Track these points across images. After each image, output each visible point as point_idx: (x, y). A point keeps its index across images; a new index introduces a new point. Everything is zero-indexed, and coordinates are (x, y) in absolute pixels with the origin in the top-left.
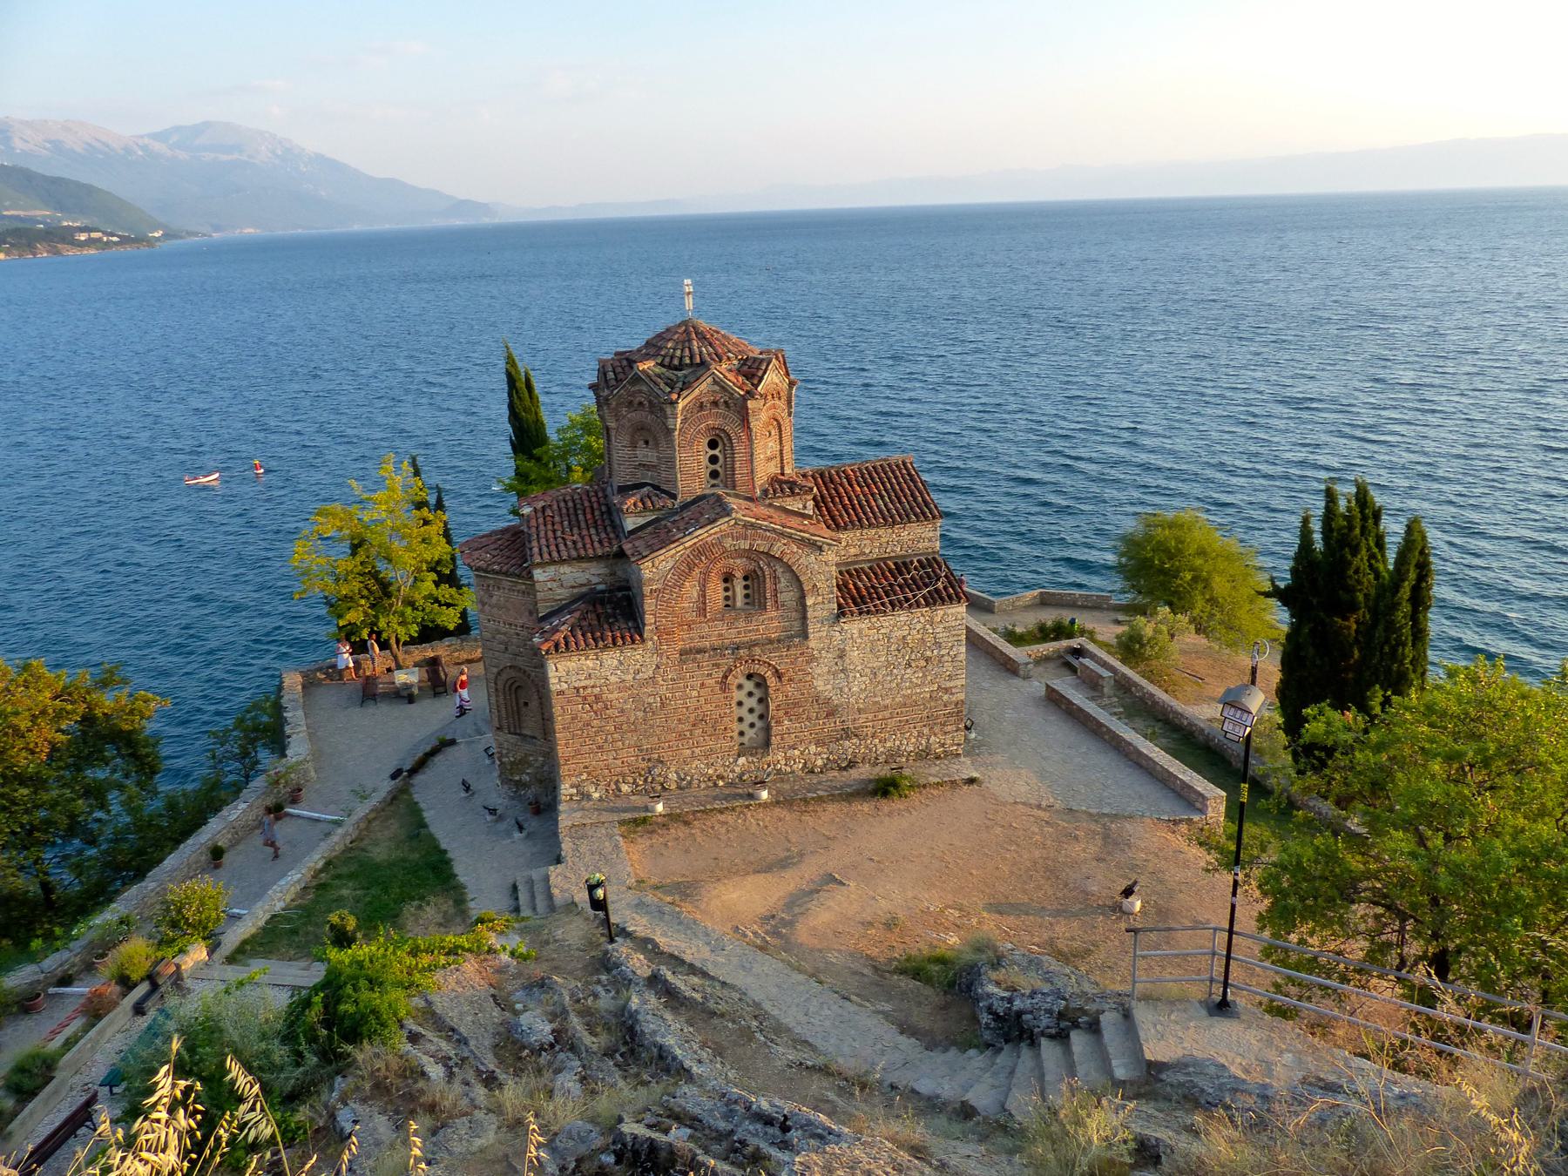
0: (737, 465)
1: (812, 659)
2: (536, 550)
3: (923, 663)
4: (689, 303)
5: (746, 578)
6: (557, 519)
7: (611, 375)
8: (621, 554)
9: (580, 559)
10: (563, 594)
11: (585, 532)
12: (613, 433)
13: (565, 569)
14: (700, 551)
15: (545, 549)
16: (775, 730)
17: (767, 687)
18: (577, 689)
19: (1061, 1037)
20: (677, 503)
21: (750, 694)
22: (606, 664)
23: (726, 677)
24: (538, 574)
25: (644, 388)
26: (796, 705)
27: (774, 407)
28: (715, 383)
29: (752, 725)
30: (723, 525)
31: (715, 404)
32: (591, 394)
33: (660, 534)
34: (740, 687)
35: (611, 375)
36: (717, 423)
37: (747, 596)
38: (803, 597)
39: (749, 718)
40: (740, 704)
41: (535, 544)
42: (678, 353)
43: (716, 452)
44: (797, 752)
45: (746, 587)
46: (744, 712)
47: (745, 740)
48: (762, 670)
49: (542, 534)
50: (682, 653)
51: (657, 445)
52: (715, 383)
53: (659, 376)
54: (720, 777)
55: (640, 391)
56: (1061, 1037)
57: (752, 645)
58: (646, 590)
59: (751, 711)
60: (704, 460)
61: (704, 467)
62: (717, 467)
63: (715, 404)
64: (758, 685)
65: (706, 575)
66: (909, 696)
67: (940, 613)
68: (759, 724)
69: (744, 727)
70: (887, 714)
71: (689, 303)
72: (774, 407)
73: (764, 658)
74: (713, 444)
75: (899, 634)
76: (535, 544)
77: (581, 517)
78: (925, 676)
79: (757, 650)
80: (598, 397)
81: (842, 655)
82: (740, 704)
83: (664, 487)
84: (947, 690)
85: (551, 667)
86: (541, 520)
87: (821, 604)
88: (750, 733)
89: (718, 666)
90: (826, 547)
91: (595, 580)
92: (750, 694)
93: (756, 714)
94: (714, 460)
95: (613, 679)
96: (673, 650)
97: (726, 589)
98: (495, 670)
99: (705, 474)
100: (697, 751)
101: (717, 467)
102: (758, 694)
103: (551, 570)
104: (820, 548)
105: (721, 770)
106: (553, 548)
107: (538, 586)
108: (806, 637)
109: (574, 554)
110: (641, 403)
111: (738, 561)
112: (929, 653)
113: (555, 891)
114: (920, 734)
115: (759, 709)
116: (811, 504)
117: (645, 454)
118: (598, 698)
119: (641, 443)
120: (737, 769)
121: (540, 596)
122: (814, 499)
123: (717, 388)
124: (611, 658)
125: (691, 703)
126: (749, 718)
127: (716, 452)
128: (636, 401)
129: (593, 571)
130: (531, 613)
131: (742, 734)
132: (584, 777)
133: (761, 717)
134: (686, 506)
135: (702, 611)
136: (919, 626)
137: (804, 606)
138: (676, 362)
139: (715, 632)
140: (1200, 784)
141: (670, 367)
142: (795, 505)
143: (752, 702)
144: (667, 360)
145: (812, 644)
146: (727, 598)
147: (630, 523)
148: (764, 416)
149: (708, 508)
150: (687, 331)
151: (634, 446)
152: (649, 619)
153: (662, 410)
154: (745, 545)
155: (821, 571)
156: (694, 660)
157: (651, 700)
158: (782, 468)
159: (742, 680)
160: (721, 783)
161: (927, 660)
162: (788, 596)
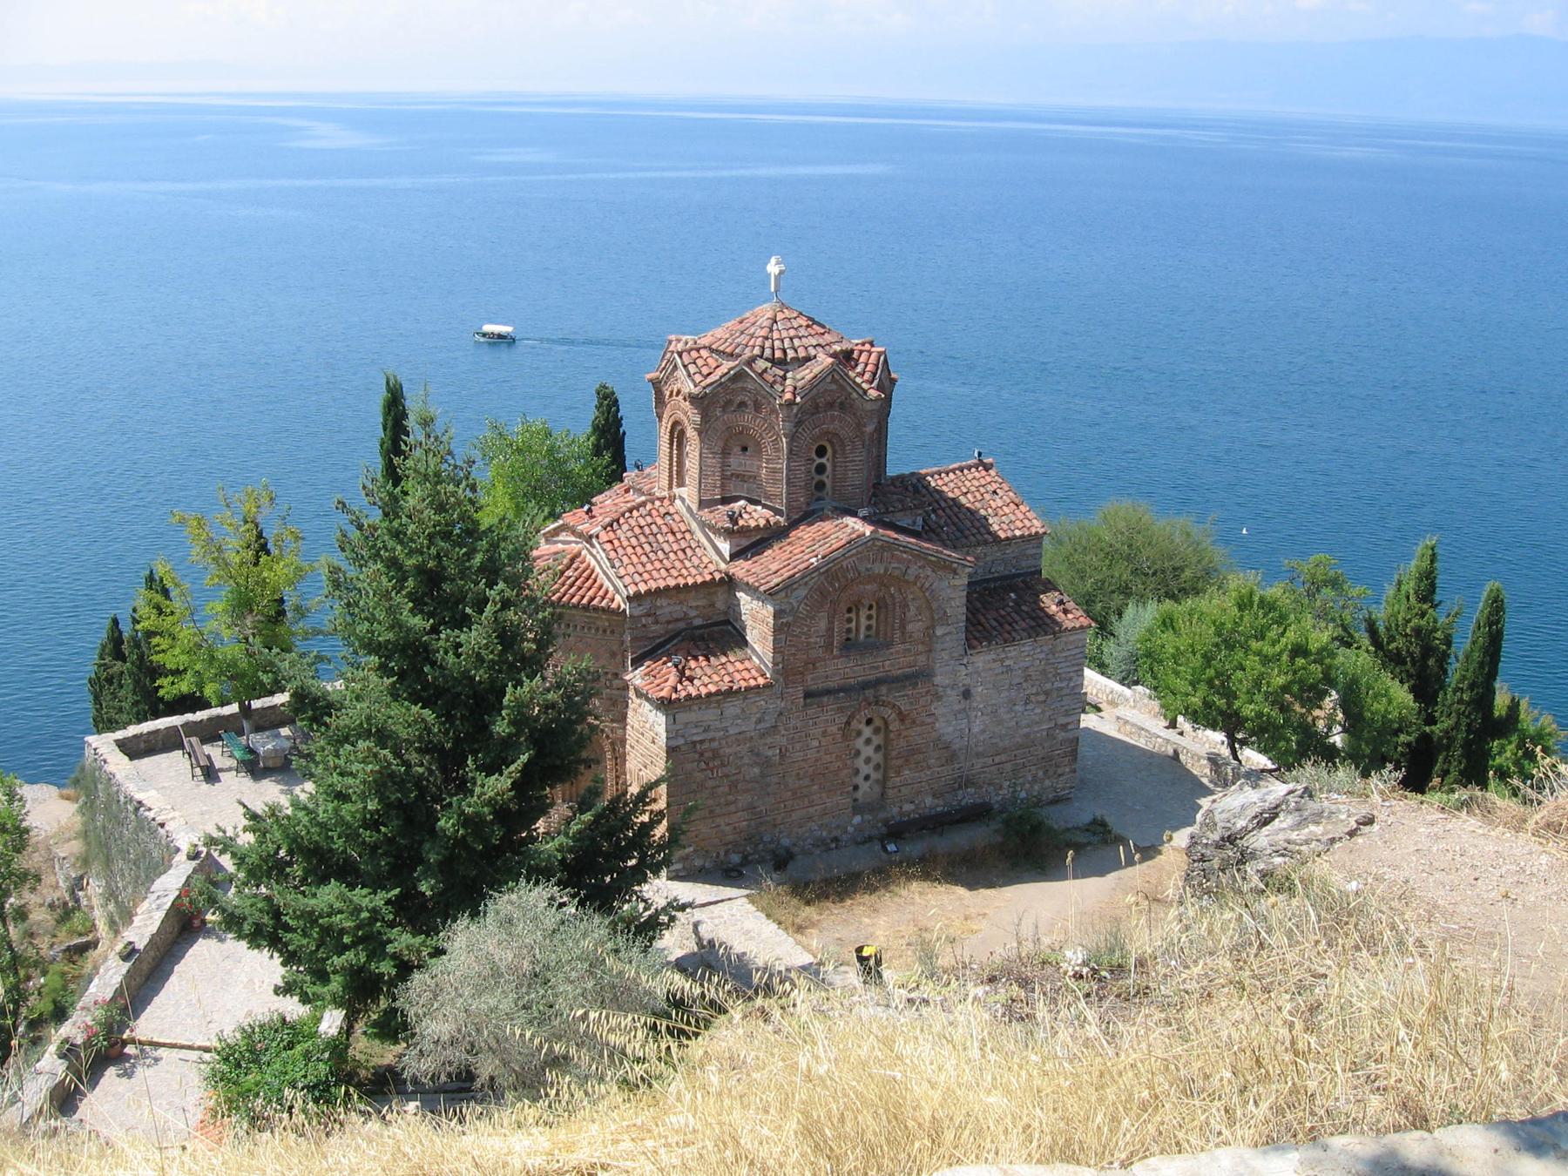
1: (938, 697)
18: (694, 743)
21: (868, 741)
22: (727, 713)
23: (848, 723)
28: (834, 381)
29: (867, 778)
31: (831, 405)
36: (834, 426)
37: (869, 628)
38: (933, 627)
39: (866, 770)
40: (858, 753)
44: (912, 807)
45: (869, 617)
49: (625, 559)
52: (834, 381)
54: (836, 839)
55: (744, 389)
62: (824, 478)
63: (831, 405)
64: (877, 731)
66: (1027, 735)
69: (859, 780)
70: (1003, 758)
74: (821, 452)
75: (1022, 664)
78: (1043, 712)
79: (884, 689)
81: (967, 694)
84: (1064, 727)
87: (951, 634)
89: (841, 710)
91: (693, 613)
92: (868, 741)
93: (871, 765)
94: (821, 469)
101: (824, 478)
102: (877, 740)
103: (647, 604)
104: (955, 572)
105: (835, 833)
110: (742, 404)
112: (1048, 686)
114: (1035, 779)
116: (920, 521)
119: (737, 449)
120: (850, 829)
123: (834, 387)
127: (823, 460)
130: (613, 655)
133: (877, 767)
135: (828, 646)
138: (778, 354)
139: (841, 670)
141: (772, 360)
143: (868, 751)
144: (768, 352)
145: (938, 680)
151: (725, 453)
154: (879, 569)
155: (953, 594)
157: (770, 753)
161: (1047, 693)
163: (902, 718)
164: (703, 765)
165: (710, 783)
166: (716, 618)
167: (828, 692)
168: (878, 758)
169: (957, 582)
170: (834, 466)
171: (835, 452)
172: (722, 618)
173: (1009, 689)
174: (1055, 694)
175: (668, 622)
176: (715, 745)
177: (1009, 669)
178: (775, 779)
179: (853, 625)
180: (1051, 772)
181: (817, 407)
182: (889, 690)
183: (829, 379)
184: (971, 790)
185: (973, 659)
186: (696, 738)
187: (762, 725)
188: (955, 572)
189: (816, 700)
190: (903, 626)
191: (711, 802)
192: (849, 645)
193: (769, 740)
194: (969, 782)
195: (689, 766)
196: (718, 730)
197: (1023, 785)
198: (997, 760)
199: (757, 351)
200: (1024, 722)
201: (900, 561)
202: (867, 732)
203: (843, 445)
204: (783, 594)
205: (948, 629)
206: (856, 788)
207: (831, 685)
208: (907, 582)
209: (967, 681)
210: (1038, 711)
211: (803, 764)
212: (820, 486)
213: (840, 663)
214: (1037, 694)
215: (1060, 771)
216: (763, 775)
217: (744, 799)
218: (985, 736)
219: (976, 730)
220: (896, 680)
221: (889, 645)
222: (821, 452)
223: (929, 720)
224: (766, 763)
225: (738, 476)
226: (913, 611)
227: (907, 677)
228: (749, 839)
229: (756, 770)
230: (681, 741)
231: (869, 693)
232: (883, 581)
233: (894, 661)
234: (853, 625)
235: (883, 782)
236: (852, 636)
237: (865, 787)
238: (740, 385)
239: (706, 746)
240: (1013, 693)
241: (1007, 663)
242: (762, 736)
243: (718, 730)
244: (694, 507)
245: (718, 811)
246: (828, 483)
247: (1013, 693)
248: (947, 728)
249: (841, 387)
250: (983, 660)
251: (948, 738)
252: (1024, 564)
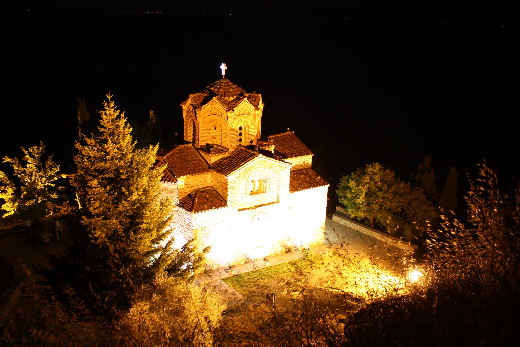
62: (241, 137)
83: (223, 145)
101: (241, 137)
119: (213, 128)
164: (205, 235)
171: (245, 129)
172: (209, 185)
175: (191, 187)
192: (252, 193)
238: (214, 106)
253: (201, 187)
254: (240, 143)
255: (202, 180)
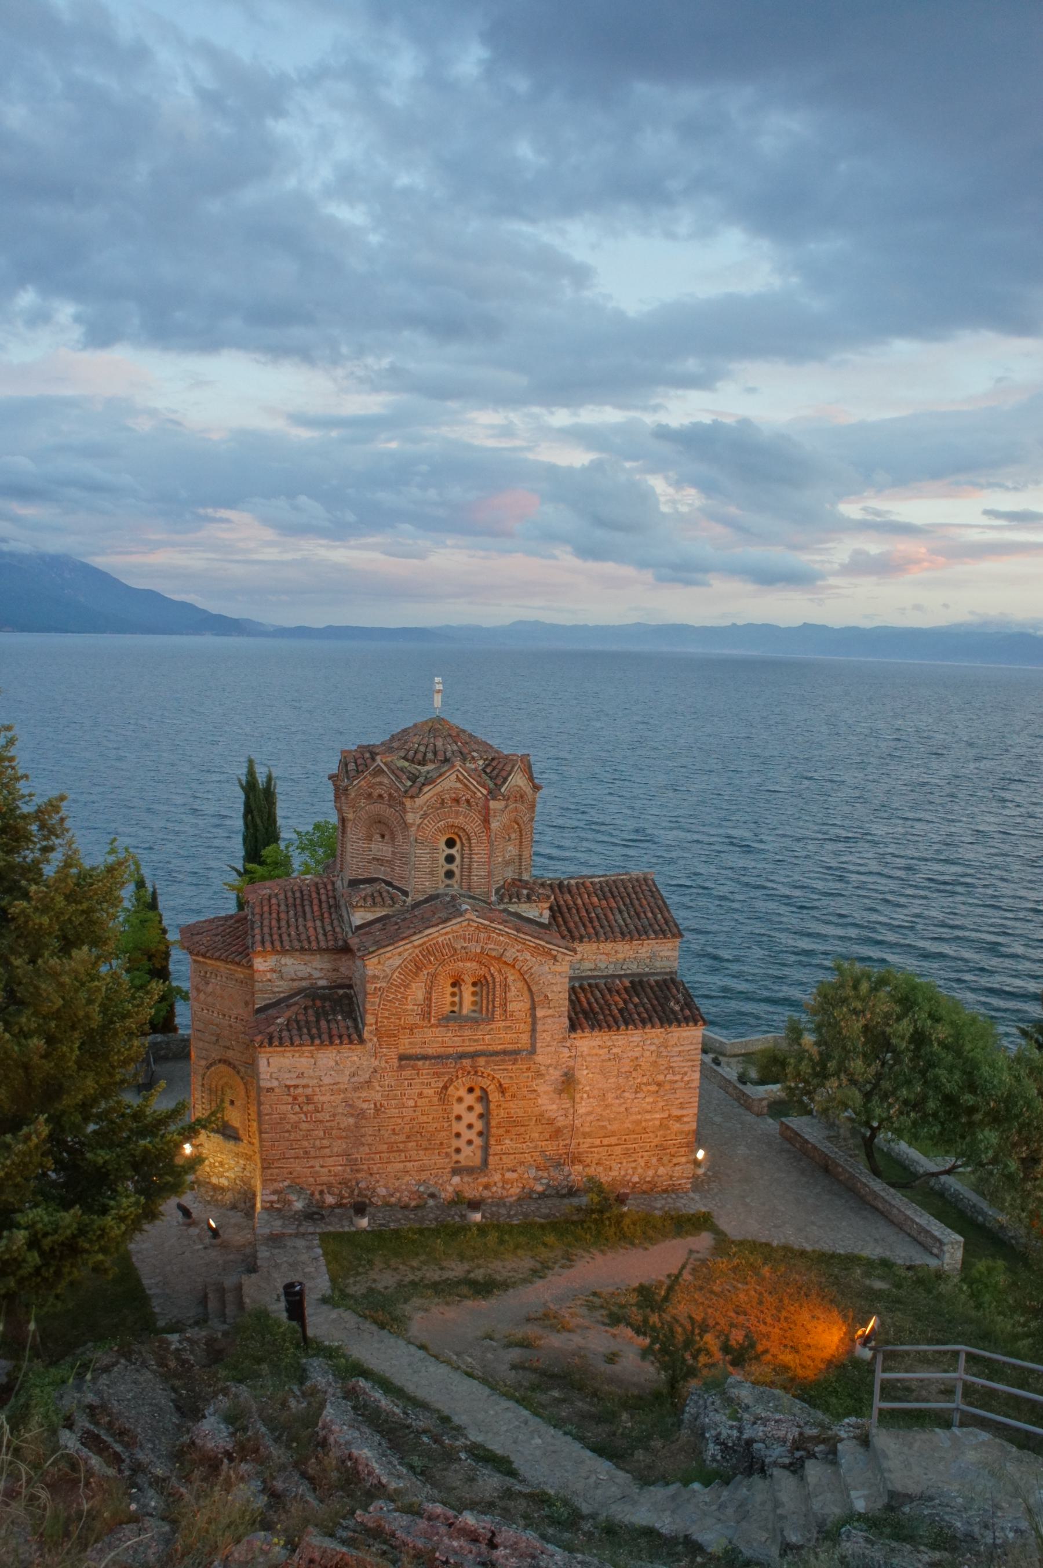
0: (475, 865)
1: (539, 1075)
2: (258, 938)
3: (654, 1088)
4: (438, 700)
5: (474, 984)
6: (283, 908)
7: (352, 766)
8: (346, 950)
9: (302, 950)
10: (282, 987)
11: (310, 924)
12: (349, 824)
13: (287, 960)
14: (429, 951)
15: (267, 937)
16: (495, 1149)
17: (488, 1102)
18: (288, 1087)
19: (796, 1468)
20: (409, 900)
21: (470, 1108)
23: (445, 1087)
24: (260, 964)
25: (386, 781)
26: (517, 1123)
27: (516, 809)
28: (458, 779)
29: (470, 1142)
30: (454, 925)
31: (457, 801)
32: (330, 782)
33: (386, 932)
34: (460, 1100)
35: (352, 766)
36: (460, 821)
37: (474, 1003)
38: (533, 1008)
39: (468, 1135)
40: (459, 1118)
41: (257, 931)
42: (422, 748)
43: (453, 851)
44: (515, 1175)
45: (474, 994)
46: (461, 1127)
47: (461, 1157)
48: (485, 1083)
49: (266, 922)
50: (402, 1058)
51: (393, 838)
52: (458, 779)
53: (401, 769)
54: (432, 1196)
55: (381, 784)
56: (796, 1468)
57: (474, 1055)
58: (370, 987)
59: (470, 1126)
60: (442, 860)
61: (444, 867)
62: (452, 867)
63: (457, 801)
65: (434, 975)
66: (638, 1122)
67: (676, 1035)
68: (478, 1141)
69: (461, 1143)
70: (613, 1140)
71: (438, 700)
72: (516, 809)
73: (489, 1071)
74: (451, 843)
75: (630, 1054)
76: (257, 931)
77: (307, 909)
79: (482, 1061)
80: (337, 788)
82: (459, 1118)
83: (396, 883)
84: (678, 1119)
85: (262, 1063)
86: (266, 908)
87: (554, 1018)
88: (467, 1151)
90: (560, 957)
91: (317, 974)
92: (470, 1108)
94: (450, 859)
95: (327, 1080)
96: (393, 1053)
97: (453, 994)
98: (203, 1063)
99: (442, 873)
100: (409, 1165)
101: (452, 867)
102: (479, 1108)
104: (555, 958)
105: (432, 1190)
106: (276, 937)
107: (257, 976)
108: (533, 1051)
109: (297, 945)
110: (380, 796)
111: (468, 964)
112: (661, 1078)
113: (247, 1300)
115: (479, 1125)
116: (547, 913)
117: (381, 848)
118: (309, 1100)
119: (377, 837)
121: (258, 986)
122: (551, 909)
123: (459, 785)
124: (327, 1057)
125: (408, 1113)
126: (468, 1135)
127: (453, 851)
128: (375, 794)
129: (315, 964)
130: (247, 1004)
131: (458, 1151)
132: (286, 1184)
133: (480, 1134)
134: (417, 905)
135: (426, 1015)
136: (653, 1048)
137: (534, 1016)
138: (420, 756)
139: (436, 1039)
140: (937, 1228)
141: (412, 761)
142: (530, 911)
143: (471, 1118)
144: (411, 753)
145: (539, 1059)
146: (453, 1004)
147: (358, 918)
148: (505, 818)
149: (438, 908)
150: (436, 727)
151: (369, 838)
152: (370, 1019)
153: (402, 804)
156: (414, 1068)
157: (365, 1106)
158: (520, 874)
159: (462, 1092)
160: (431, 1202)
161: (659, 1085)
162: (518, 1006)
163: (502, 1089)
165: (304, 1126)
166: (339, 981)
167: (425, 1058)
168: (479, 1125)
169: (558, 968)
170: (462, 858)
171: (462, 844)
172: (347, 982)
173: (618, 1076)
174: (667, 1087)
175: (293, 980)
176: (309, 1091)
177: (617, 1058)
178: (370, 1131)
179: (457, 999)
180: (665, 1159)
181: (443, 802)
182: (487, 1062)
183: (454, 777)
184: (579, 1168)
185: (577, 1043)
186: (288, 1083)
187: (356, 1079)
188: (555, 958)
189: (412, 1062)
190: (505, 1004)
191: (305, 1143)
192: (453, 1018)
193: (364, 1094)
194: (576, 1159)
195: (284, 1107)
196: (311, 1077)
197: (634, 1168)
198: (606, 1141)
199: (402, 753)
200: (634, 1110)
201: (498, 943)
202: (470, 1099)
203: (469, 839)
204: (375, 960)
205: (551, 1012)
206: (458, 1151)
207: (430, 1051)
208: (505, 963)
209: (571, 1063)
210: (650, 1099)
211: (399, 1121)
212: (449, 874)
213: (439, 1031)
214: (649, 1084)
215: (675, 1161)
216: (357, 1126)
217: (339, 1146)
218: (589, 1118)
219: (582, 1111)
220: (496, 1053)
221: (491, 1019)
222: (451, 843)
223: (532, 1096)
224: (361, 1115)
225: (378, 860)
226: (513, 992)
227: (505, 1052)
228: (345, 1183)
229: (351, 1120)
230: (275, 1083)
231: (466, 1062)
232: (481, 958)
233: (497, 1035)
234: (457, 999)
235: (486, 1148)
236: (456, 1009)
237: (467, 1151)
238: (378, 780)
239: (300, 1090)
240: (621, 1080)
241: (614, 1050)
242: (356, 1089)
243: (311, 1077)
244: (346, 885)
245: (313, 1153)
246: (457, 871)
247: (621, 1080)
248: (549, 1104)
249: (466, 785)
250: (589, 1043)
251: (553, 1115)
252: (658, 964)
253: (322, 983)
254: (448, 882)
255: (326, 966)
